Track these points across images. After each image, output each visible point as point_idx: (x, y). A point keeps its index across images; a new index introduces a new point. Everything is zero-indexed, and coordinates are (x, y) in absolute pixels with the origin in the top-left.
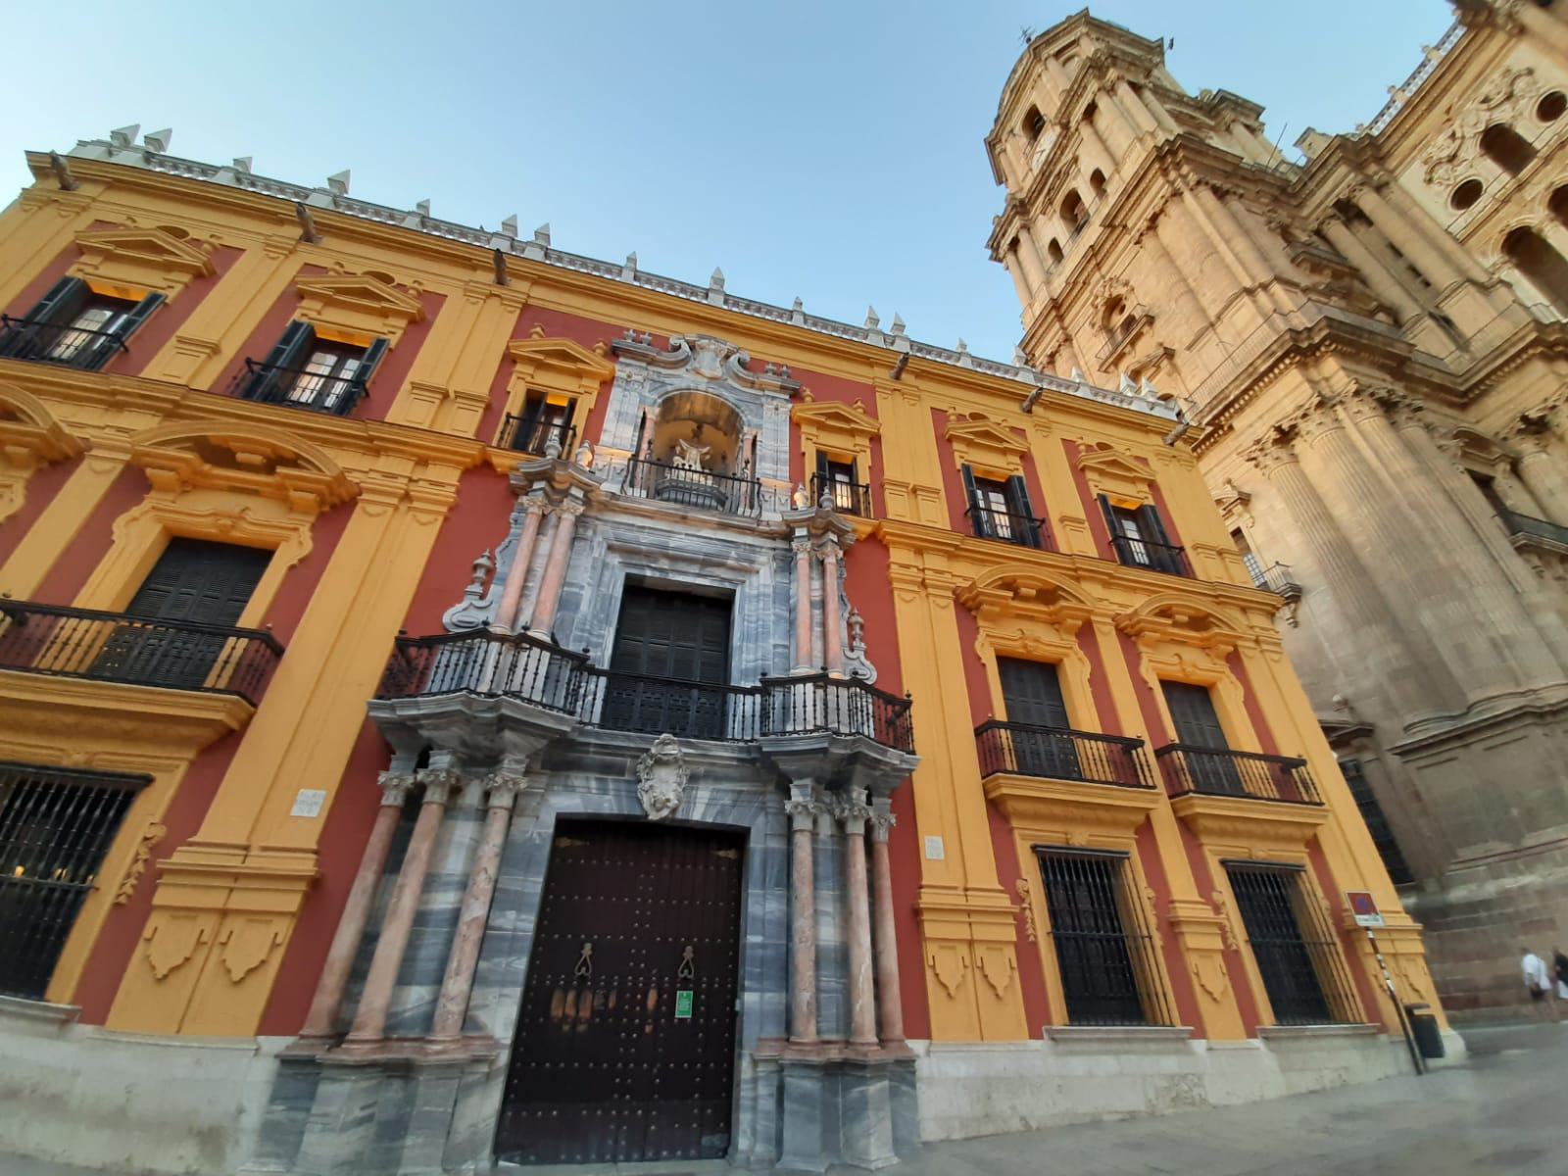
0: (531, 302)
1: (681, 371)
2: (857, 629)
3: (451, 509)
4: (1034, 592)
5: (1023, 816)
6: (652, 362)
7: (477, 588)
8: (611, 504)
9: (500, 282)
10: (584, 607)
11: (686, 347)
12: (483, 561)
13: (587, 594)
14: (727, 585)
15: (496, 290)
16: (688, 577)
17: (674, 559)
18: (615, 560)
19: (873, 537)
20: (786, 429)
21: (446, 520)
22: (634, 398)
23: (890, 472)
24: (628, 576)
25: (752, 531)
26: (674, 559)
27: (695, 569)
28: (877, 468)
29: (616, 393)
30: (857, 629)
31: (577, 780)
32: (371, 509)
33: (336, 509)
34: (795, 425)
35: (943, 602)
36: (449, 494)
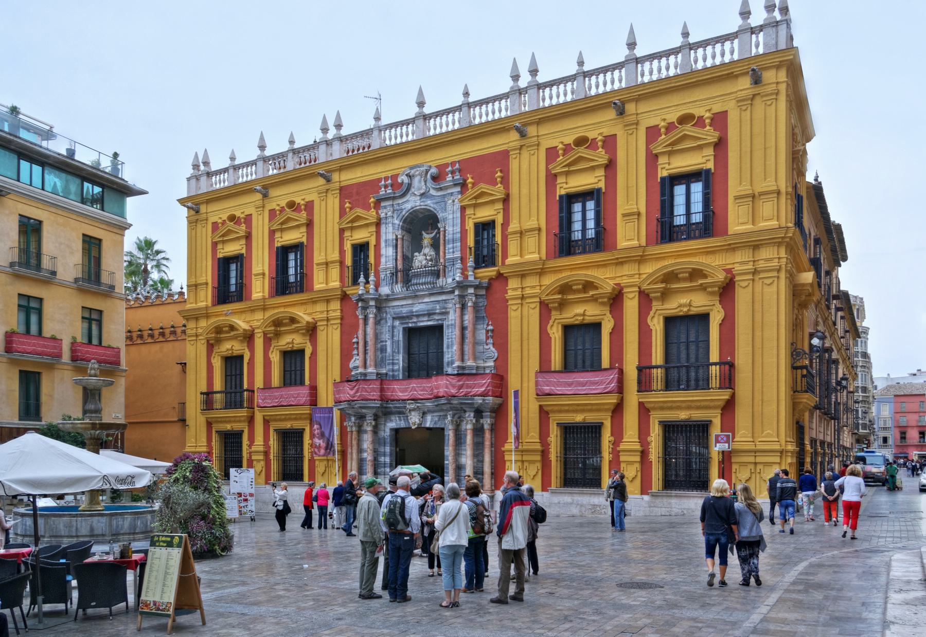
0: (343, 184)
1: (408, 197)
2: (490, 334)
3: (342, 319)
4: (580, 287)
5: (554, 412)
6: (394, 198)
7: (355, 352)
8: (388, 299)
9: (328, 180)
10: (389, 350)
11: (406, 180)
12: (355, 340)
13: (389, 343)
14: (440, 322)
15: (327, 187)
16: (425, 322)
17: (418, 316)
18: (397, 323)
19: (500, 275)
20: (459, 215)
21: (341, 324)
22: (390, 229)
23: (513, 226)
24: (404, 329)
25: (444, 293)
26: (418, 316)
27: (426, 318)
28: (505, 225)
29: (383, 228)
30: (490, 334)
31: (393, 418)
32: (321, 328)
33: (312, 331)
34: (463, 209)
35: (533, 306)
36: (338, 313)
